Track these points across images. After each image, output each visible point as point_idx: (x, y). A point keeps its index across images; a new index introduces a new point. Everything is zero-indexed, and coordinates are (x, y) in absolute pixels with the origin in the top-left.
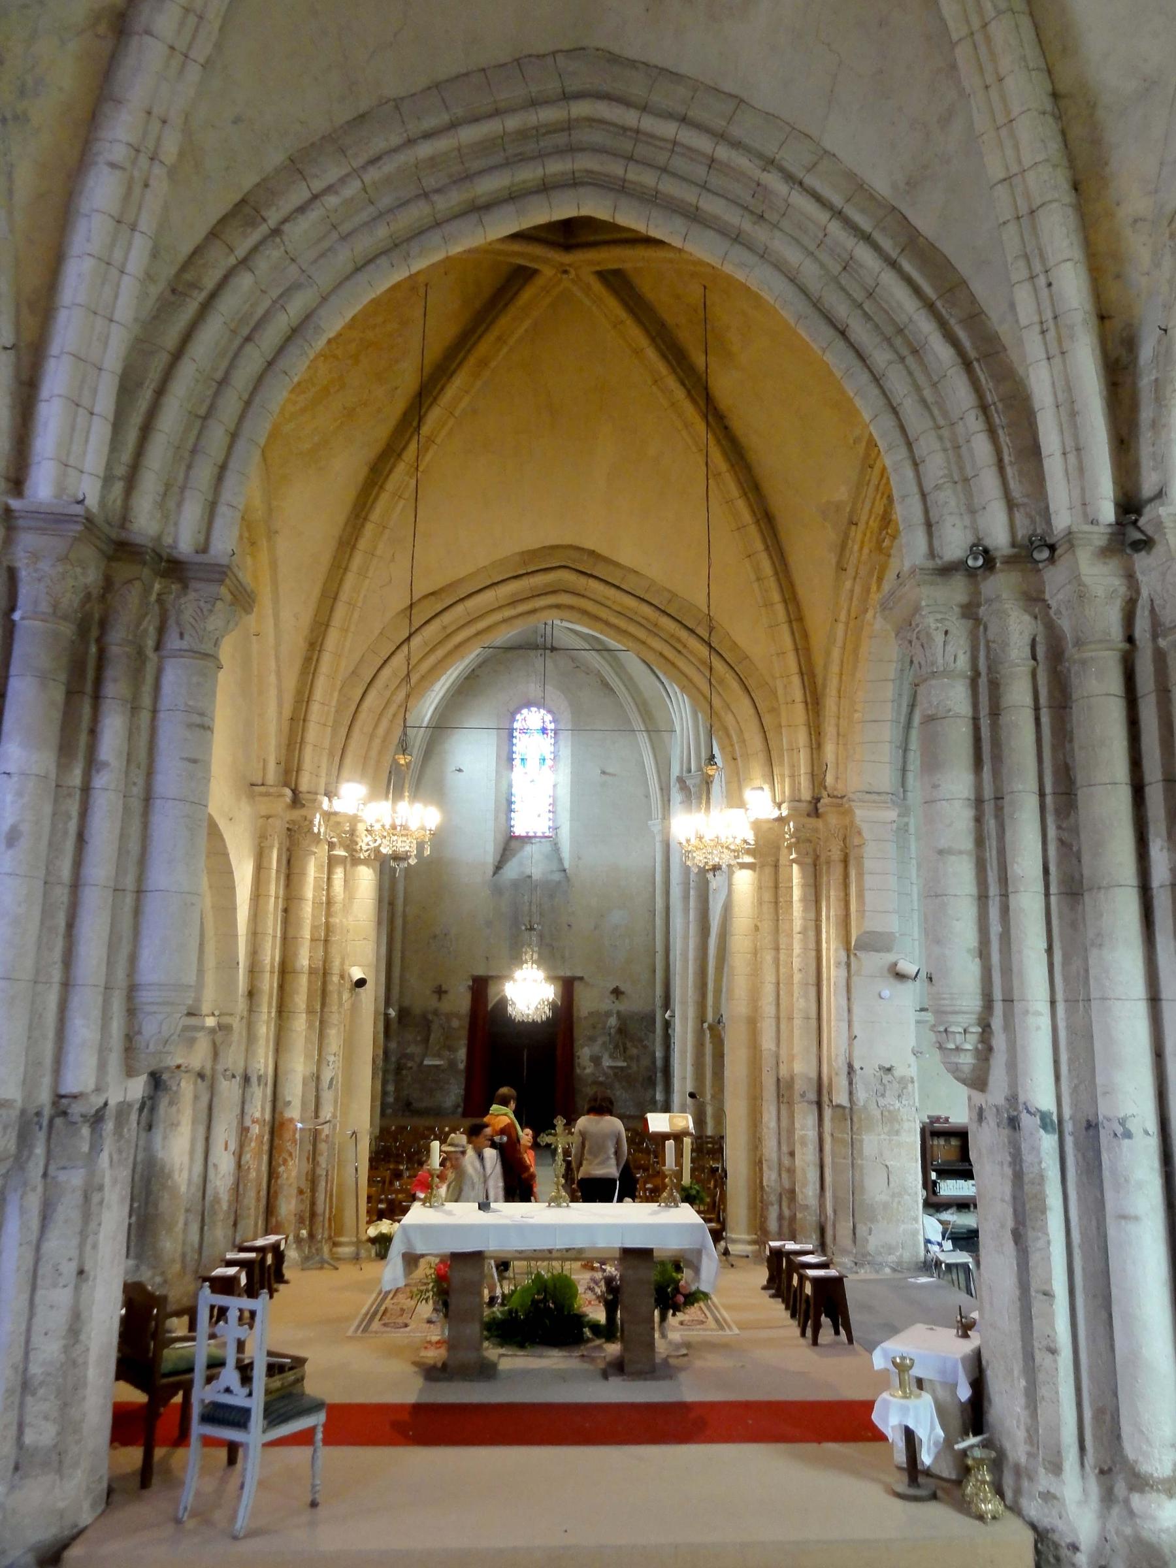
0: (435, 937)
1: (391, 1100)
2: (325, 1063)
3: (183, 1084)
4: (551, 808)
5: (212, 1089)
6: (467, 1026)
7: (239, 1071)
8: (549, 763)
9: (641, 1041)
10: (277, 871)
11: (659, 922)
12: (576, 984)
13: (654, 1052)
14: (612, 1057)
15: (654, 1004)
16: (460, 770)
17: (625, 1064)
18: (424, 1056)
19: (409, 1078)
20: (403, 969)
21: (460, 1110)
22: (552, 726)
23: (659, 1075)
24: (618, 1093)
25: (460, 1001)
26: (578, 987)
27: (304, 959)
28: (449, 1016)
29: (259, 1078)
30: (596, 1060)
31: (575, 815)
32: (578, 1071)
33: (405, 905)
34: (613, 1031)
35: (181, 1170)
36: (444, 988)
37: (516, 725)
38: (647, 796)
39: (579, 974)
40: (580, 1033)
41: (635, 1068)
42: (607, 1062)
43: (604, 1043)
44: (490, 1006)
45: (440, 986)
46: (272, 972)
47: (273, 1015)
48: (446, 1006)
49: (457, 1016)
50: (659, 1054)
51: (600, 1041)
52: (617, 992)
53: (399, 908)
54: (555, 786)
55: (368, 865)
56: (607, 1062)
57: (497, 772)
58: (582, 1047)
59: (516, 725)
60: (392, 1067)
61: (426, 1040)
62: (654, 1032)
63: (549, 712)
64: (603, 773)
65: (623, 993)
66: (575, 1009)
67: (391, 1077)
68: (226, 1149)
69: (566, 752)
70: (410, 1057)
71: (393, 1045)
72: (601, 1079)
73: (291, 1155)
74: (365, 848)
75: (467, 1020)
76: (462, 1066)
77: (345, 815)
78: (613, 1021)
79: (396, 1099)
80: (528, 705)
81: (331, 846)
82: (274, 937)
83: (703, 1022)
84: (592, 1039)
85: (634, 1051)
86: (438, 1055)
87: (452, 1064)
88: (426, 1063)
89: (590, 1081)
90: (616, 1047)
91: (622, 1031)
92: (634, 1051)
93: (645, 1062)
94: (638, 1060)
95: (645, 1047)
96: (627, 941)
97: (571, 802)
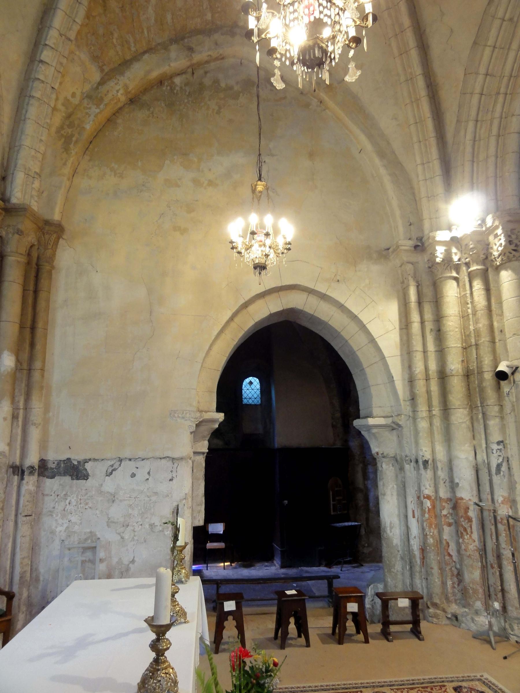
2: (490, 451)
3: (384, 466)
5: (402, 469)
7: (413, 458)
10: (420, 303)
27: (455, 364)
29: (426, 463)
35: (391, 528)
46: (427, 379)
47: (436, 411)
55: (506, 269)
68: (414, 517)
73: (465, 530)
74: (496, 254)
77: (466, 236)
81: (468, 265)
82: (425, 352)
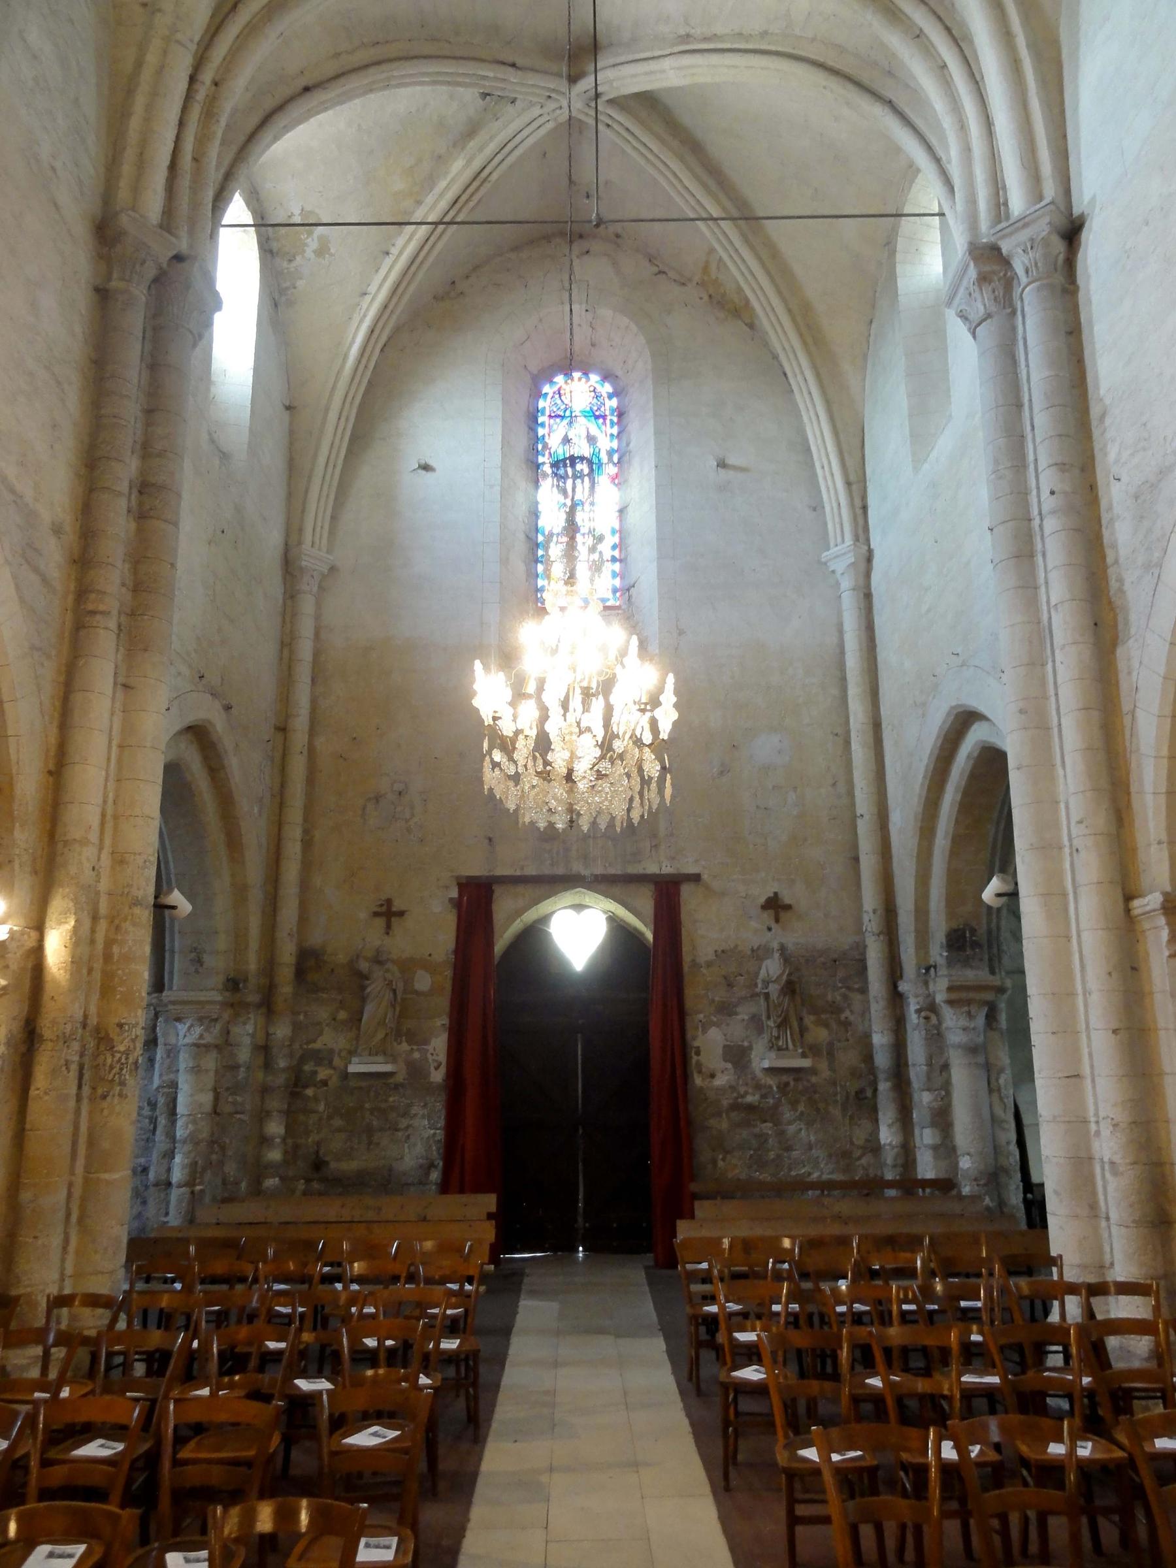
0: (377, 799)
1: (275, 1155)
4: (616, 553)
6: (448, 986)
8: (612, 470)
9: (835, 1009)
11: (859, 752)
12: (686, 890)
13: (867, 1036)
14: (773, 1046)
15: (860, 931)
16: (426, 468)
17: (806, 1063)
18: (352, 1053)
19: (321, 1107)
20: (307, 865)
21: (435, 1176)
22: (614, 402)
23: (884, 1086)
24: (792, 1129)
25: (433, 932)
26: (688, 895)
28: (408, 966)
30: (737, 1056)
31: (669, 543)
32: (698, 1081)
33: (312, 732)
34: (774, 989)
36: (397, 905)
37: (541, 404)
38: (817, 507)
39: (692, 869)
40: (700, 994)
41: (826, 1073)
42: (762, 1059)
43: (755, 1018)
44: (500, 946)
45: (389, 902)
48: (401, 944)
49: (427, 965)
50: (880, 1039)
51: (744, 1013)
52: (775, 906)
53: (299, 737)
54: (622, 511)
56: (762, 1059)
57: (504, 472)
58: (705, 1031)
59: (541, 404)
60: (280, 1080)
61: (356, 1019)
62: (864, 990)
63: (605, 378)
64: (722, 464)
65: (788, 907)
66: (685, 949)
67: (276, 1103)
69: (643, 435)
70: (322, 1058)
71: (282, 1031)
72: (749, 1099)
75: (449, 973)
76: (438, 1076)
78: (772, 967)
79: (292, 1153)
80: (568, 365)
83: (1128, 898)
84: (726, 1010)
85: (820, 1035)
86: (381, 1050)
87: (416, 1071)
88: (352, 1069)
89: (725, 1103)
90: (783, 1024)
91: (790, 988)
92: (820, 1035)
93: (849, 1058)
94: (831, 1054)
95: (846, 1024)
96: (792, 797)
97: (659, 521)
